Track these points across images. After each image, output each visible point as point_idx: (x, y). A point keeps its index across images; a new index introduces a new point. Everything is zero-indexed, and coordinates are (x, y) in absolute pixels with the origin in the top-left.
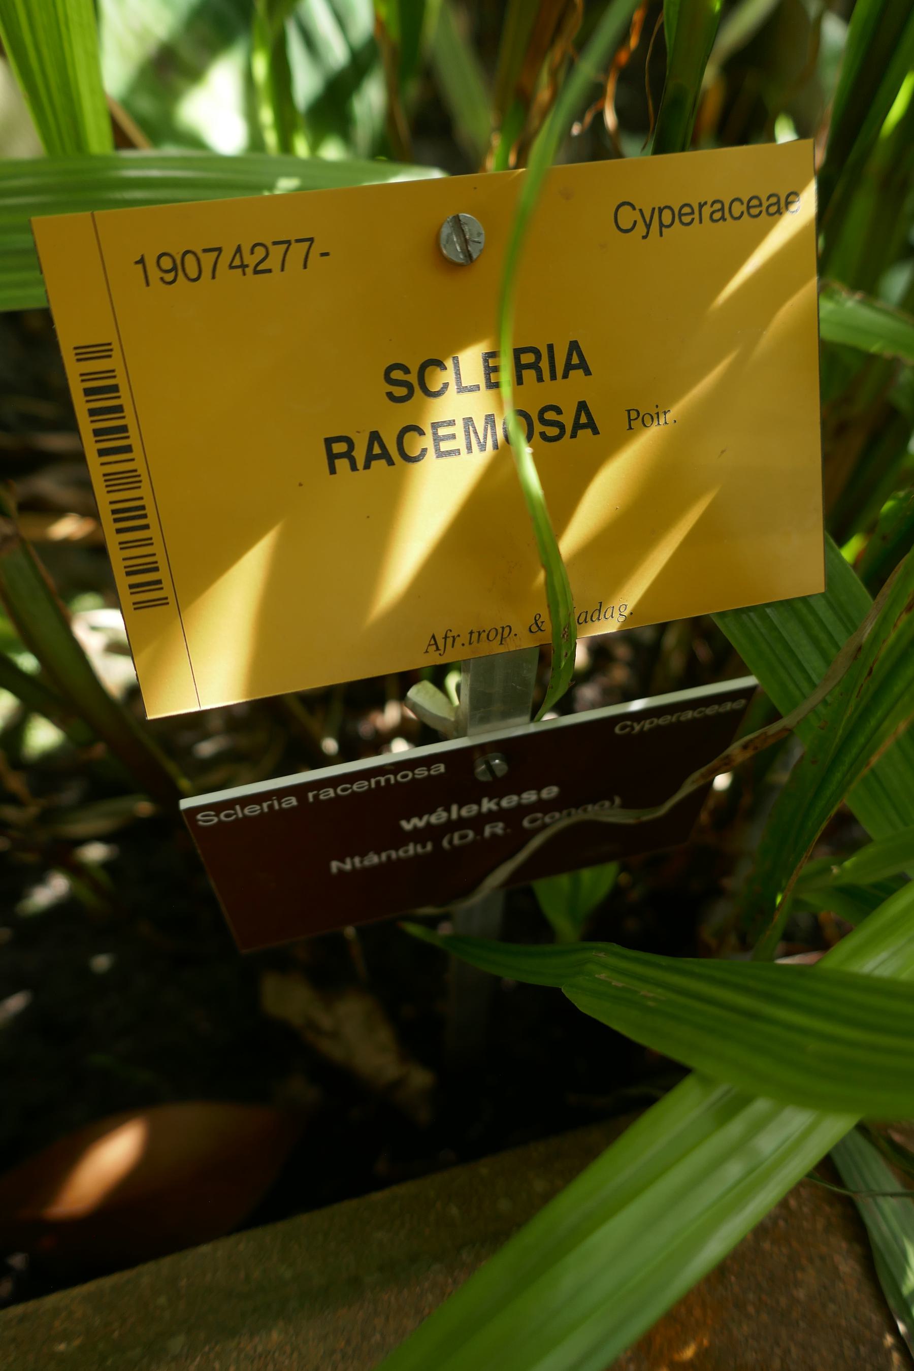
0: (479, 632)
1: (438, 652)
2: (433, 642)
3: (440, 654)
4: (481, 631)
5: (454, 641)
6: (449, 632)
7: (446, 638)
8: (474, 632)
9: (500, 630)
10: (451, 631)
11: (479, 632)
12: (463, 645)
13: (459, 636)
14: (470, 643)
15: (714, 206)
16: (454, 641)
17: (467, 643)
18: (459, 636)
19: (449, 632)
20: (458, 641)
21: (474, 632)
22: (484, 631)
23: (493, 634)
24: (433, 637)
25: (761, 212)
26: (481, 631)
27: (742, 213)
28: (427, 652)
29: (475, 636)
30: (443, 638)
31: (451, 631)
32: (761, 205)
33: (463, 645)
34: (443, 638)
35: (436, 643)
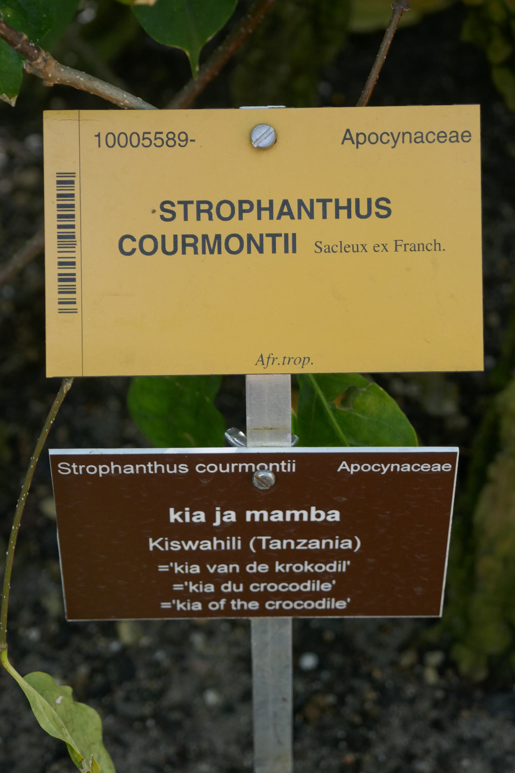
0: (290, 358)
1: (263, 366)
2: (260, 359)
3: (264, 368)
4: (275, 358)
5: (274, 360)
6: (271, 355)
7: (269, 358)
8: (286, 358)
9: (303, 359)
10: (272, 354)
11: (290, 358)
12: (279, 364)
13: (277, 358)
14: (283, 364)
15: (417, 134)
16: (274, 360)
17: (281, 363)
18: (277, 358)
19: (271, 355)
20: (276, 361)
21: (286, 358)
22: (293, 358)
23: (298, 360)
24: (262, 356)
25: (446, 140)
26: (275, 358)
27: (434, 140)
28: (256, 365)
29: (287, 360)
30: (267, 358)
31: (272, 354)
32: (446, 136)
33: (279, 364)
34: (267, 358)
35: (262, 361)
